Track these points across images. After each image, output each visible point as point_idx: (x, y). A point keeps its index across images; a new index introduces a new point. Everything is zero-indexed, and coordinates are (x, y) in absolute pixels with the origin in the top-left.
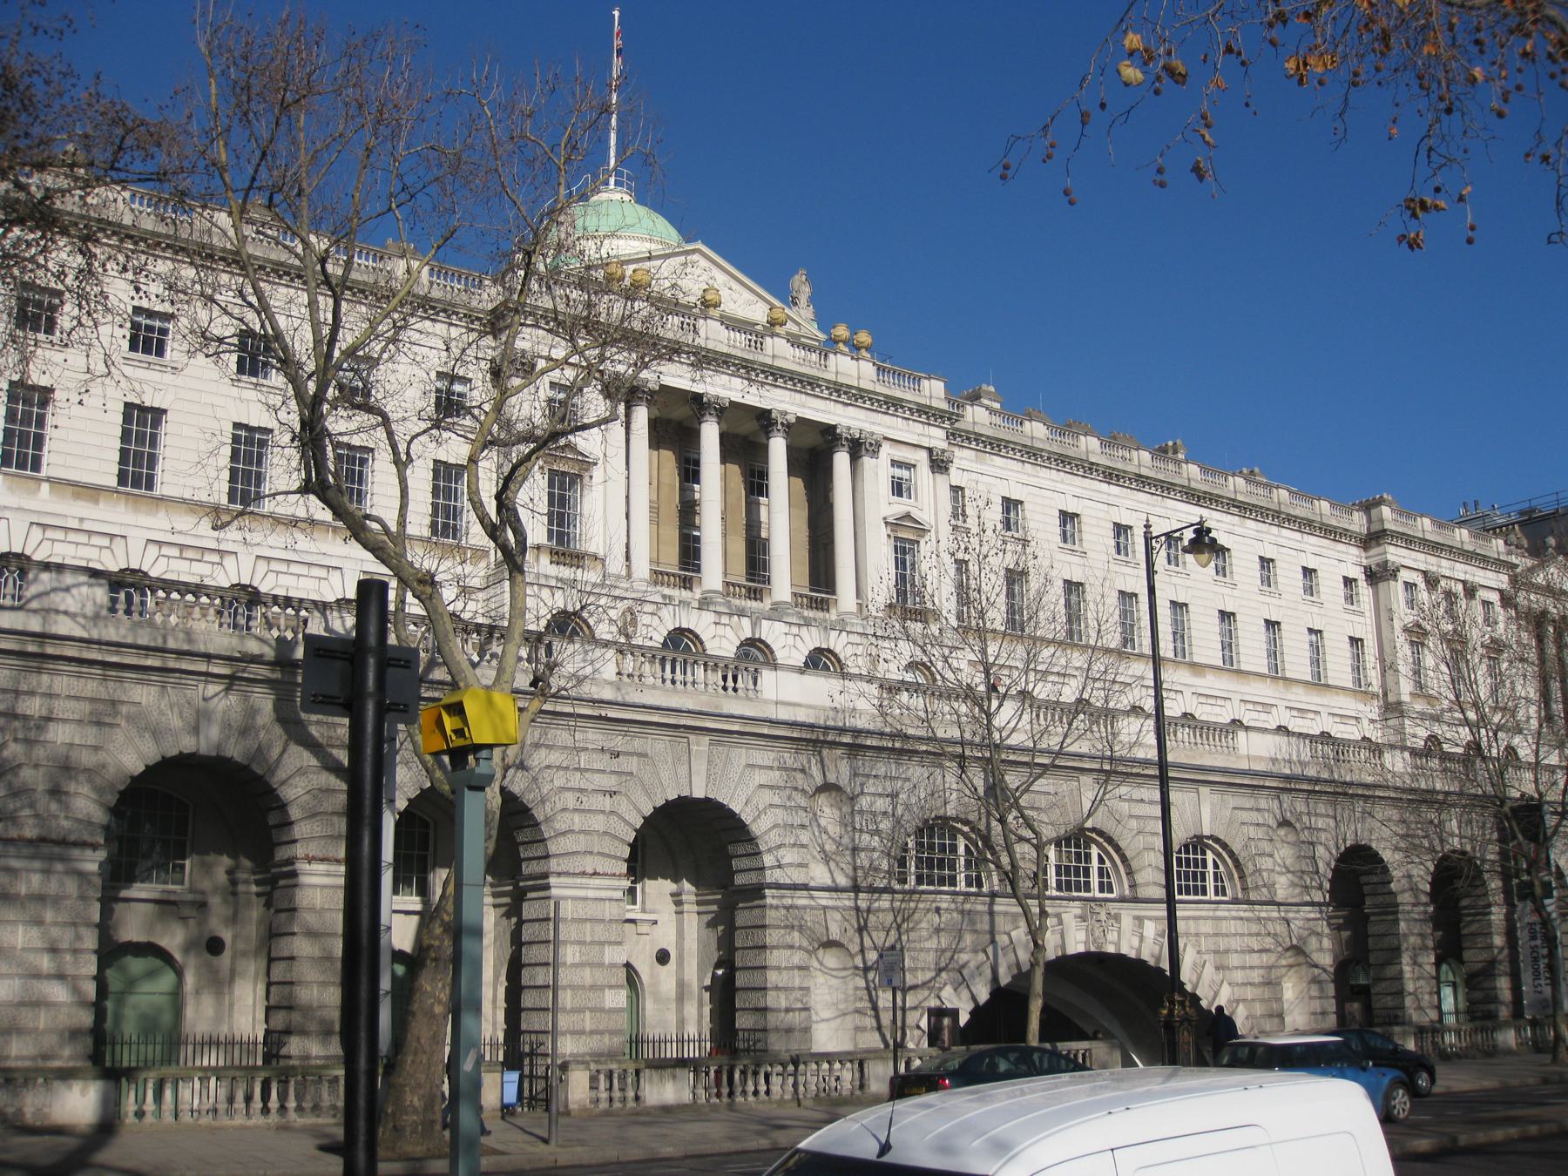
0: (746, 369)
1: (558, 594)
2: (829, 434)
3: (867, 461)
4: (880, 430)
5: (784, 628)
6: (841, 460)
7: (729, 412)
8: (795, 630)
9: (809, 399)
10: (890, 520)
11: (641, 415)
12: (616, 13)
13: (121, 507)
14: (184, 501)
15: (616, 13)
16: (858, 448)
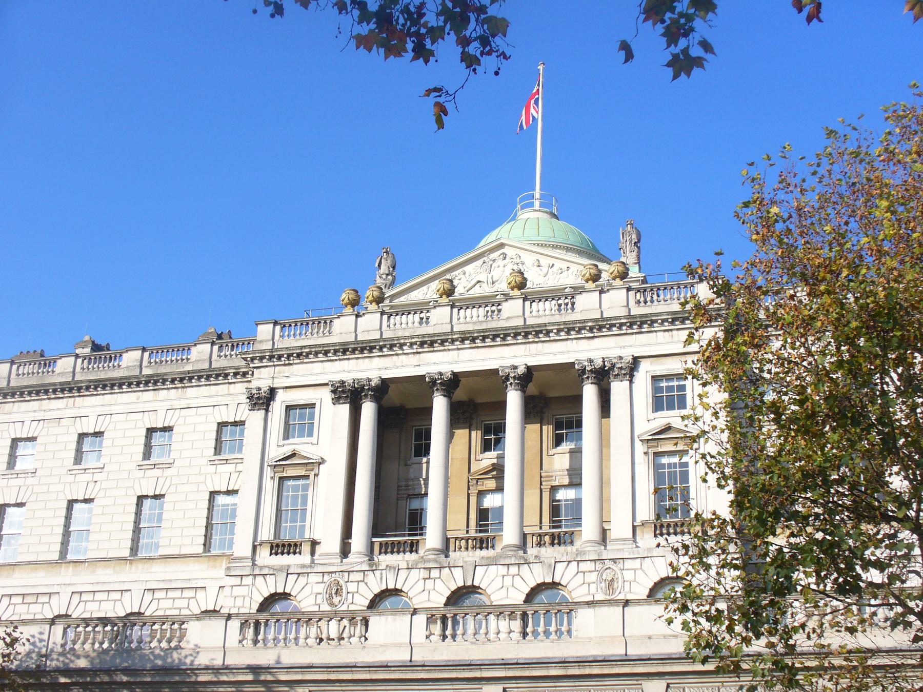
0: (469, 338)
1: (271, 579)
2: (571, 375)
3: (618, 388)
4: (628, 354)
5: (503, 570)
6: (590, 393)
7: (451, 384)
8: (514, 570)
9: (545, 344)
10: (646, 437)
11: (368, 410)
12: (541, 67)
13: (109, 571)
14: (29, 563)
15: (541, 67)
16: (603, 376)
